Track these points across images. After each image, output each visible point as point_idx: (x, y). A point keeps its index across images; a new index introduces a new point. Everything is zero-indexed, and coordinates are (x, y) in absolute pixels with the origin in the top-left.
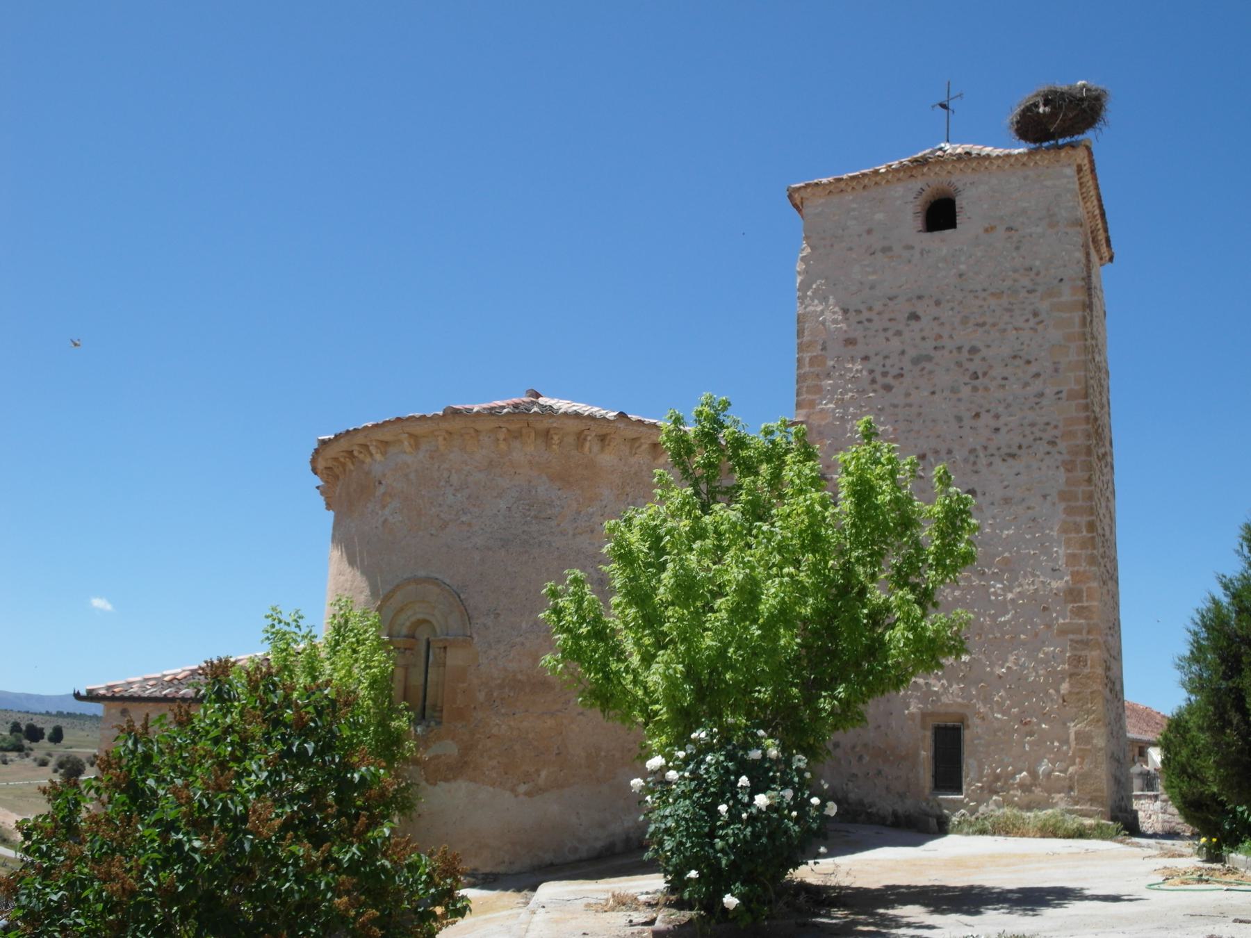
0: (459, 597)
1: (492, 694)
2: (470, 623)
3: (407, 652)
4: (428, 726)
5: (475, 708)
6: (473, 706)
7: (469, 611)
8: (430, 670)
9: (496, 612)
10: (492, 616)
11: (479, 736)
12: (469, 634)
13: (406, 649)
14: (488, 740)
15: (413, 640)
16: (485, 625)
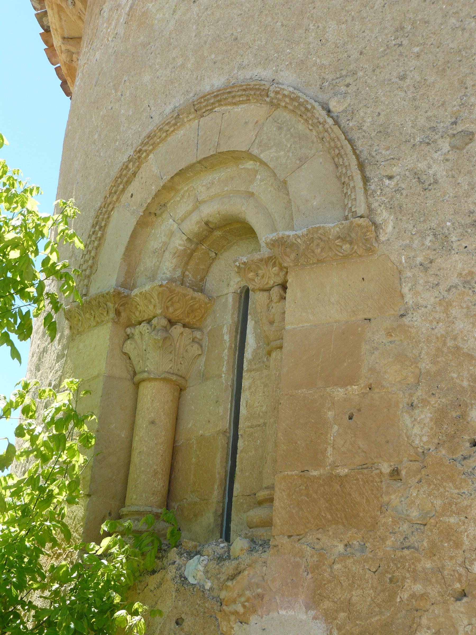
0: (329, 111)
1: (463, 416)
2: (366, 180)
3: (177, 330)
4: (220, 559)
5: (395, 474)
6: (386, 468)
7: (359, 144)
8: (246, 383)
9: (460, 128)
10: (445, 146)
11: (418, 588)
12: (361, 210)
13: (172, 323)
14: (460, 606)
15: (199, 295)
16: (417, 176)
